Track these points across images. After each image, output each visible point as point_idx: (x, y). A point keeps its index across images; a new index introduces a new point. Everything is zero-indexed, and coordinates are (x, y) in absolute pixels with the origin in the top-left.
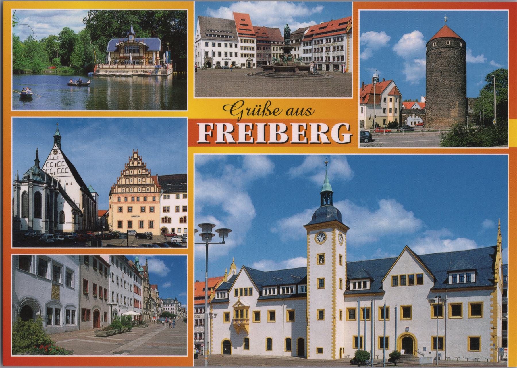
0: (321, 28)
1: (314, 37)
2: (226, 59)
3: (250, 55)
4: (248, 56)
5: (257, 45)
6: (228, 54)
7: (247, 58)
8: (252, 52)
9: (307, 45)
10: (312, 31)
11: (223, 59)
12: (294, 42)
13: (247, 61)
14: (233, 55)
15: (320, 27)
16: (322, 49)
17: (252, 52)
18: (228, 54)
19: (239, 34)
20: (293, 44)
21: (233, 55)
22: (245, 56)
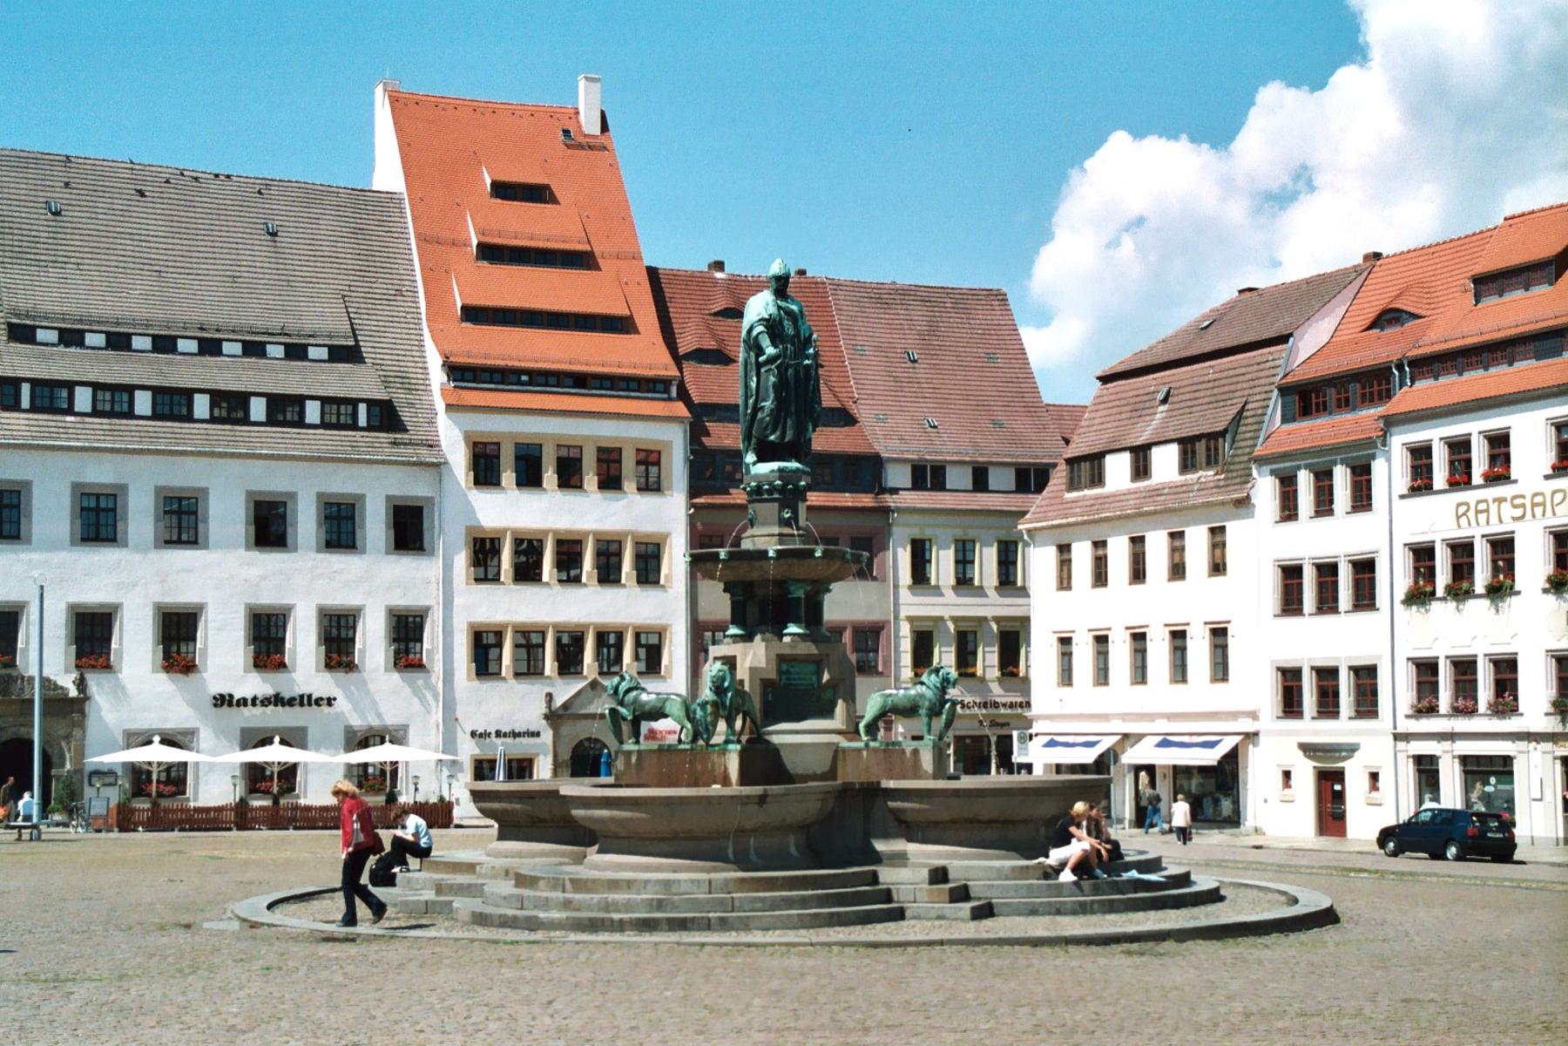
3: (609, 641)
4: (569, 661)
5: (697, 515)
6: (303, 641)
7: (565, 691)
10: (1388, 317)
11: (223, 701)
12: (1165, 461)
13: (555, 717)
14: (372, 640)
15: (1484, 266)
16: (1503, 547)
18: (303, 641)
19: (459, 373)
20: (1157, 491)
21: (372, 640)
22: (530, 669)
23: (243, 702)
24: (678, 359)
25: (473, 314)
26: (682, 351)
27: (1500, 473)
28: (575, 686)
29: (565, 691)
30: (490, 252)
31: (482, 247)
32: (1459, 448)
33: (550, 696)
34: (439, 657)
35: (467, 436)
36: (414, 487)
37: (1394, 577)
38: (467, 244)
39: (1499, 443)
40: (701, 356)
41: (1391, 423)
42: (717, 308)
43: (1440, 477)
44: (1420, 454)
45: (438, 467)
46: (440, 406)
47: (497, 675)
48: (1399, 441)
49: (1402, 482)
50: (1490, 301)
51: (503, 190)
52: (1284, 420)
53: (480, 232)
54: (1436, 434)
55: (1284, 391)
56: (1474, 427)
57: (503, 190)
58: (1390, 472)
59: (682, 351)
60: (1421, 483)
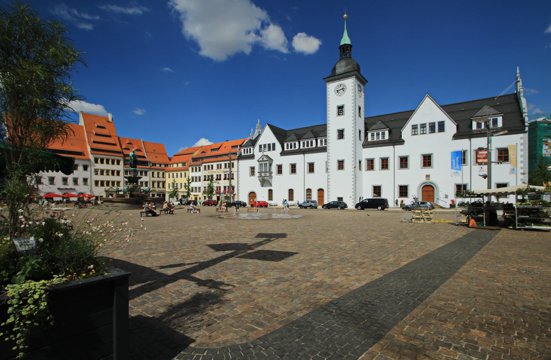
0: (212, 150)
1: (205, 160)
2: (67, 189)
4: (108, 185)
7: (107, 188)
8: (115, 178)
9: (196, 171)
10: (203, 152)
11: (59, 189)
14: (80, 181)
17: (115, 178)
19: (93, 149)
22: (102, 185)
23: (62, 189)
24: (122, 149)
25: (94, 142)
26: (123, 148)
27: (212, 168)
28: (109, 187)
29: (107, 188)
30: (97, 134)
31: (95, 134)
32: (209, 166)
33: (105, 189)
34: (90, 184)
35: (94, 157)
36: (86, 163)
37: (202, 178)
38: (93, 133)
39: (212, 166)
40: (125, 149)
41: (203, 163)
42: (127, 143)
43: (207, 169)
44: (205, 166)
45: (89, 160)
46: (90, 153)
47: (98, 186)
48: (203, 165)
49: (203, 169)
50: (212, 152)
51: (98, 127)
52: (193, 162)
53: (95, 132)
54: (207, 164)
55: (193, 159)
56: (210, 164)
57: (98, 127)
58: (202, 168)
59: (123, 148)
60: (205, 169)
